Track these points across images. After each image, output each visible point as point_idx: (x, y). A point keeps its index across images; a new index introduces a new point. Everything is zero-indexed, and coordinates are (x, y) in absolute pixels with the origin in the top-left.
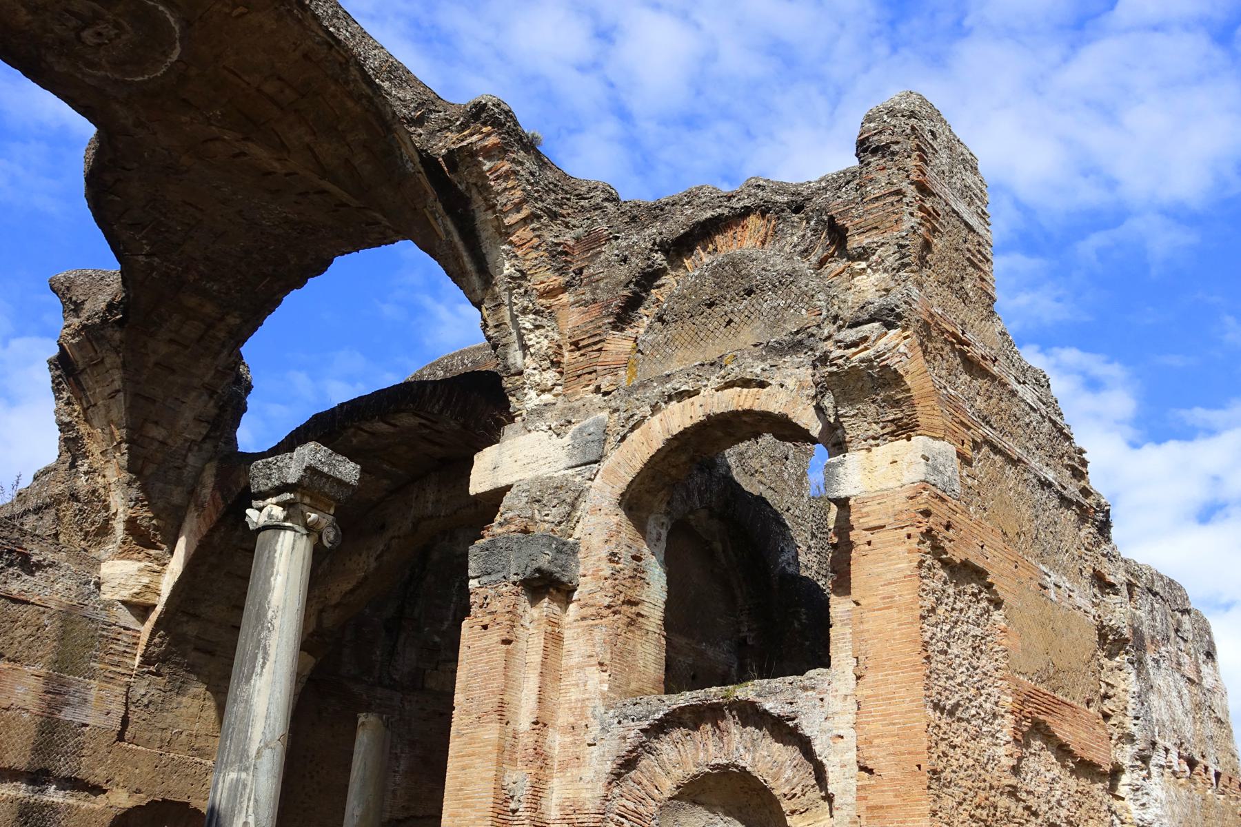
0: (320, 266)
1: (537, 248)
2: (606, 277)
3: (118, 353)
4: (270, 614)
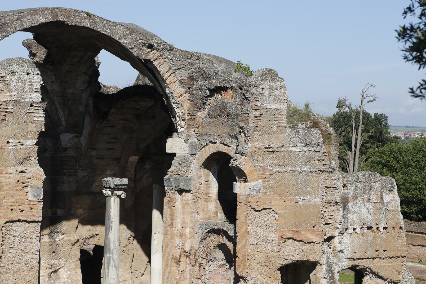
4: (111, 218)
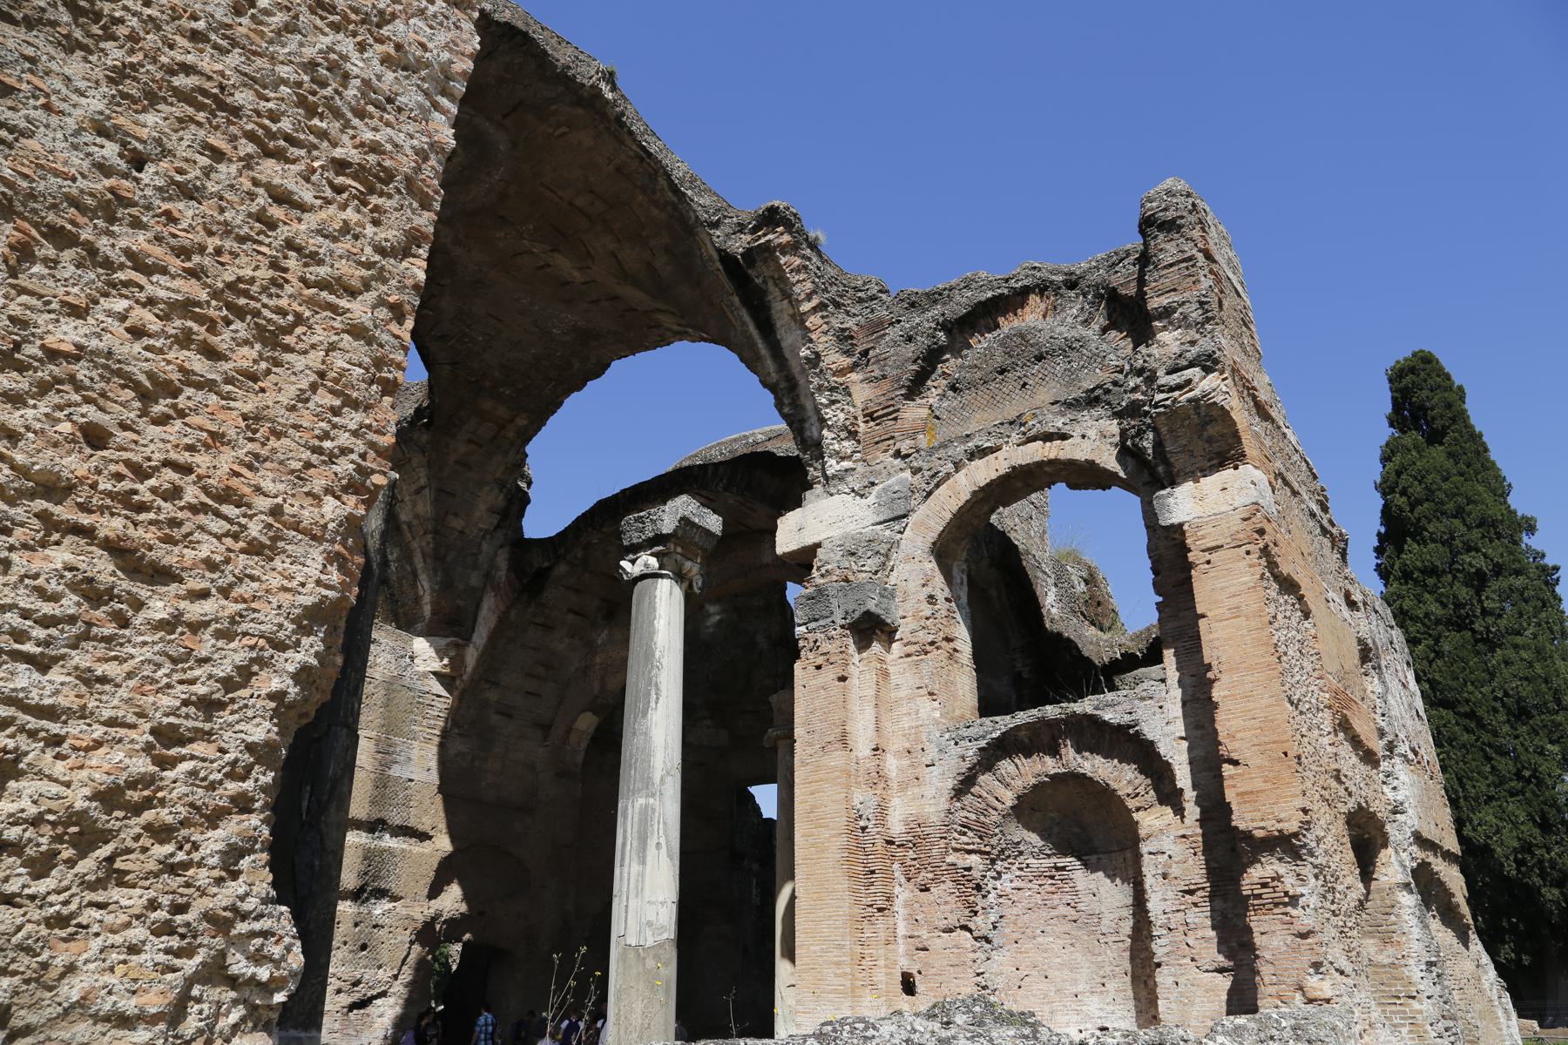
0: (599, 370)
1: (825, 333)
4: (657, 654)
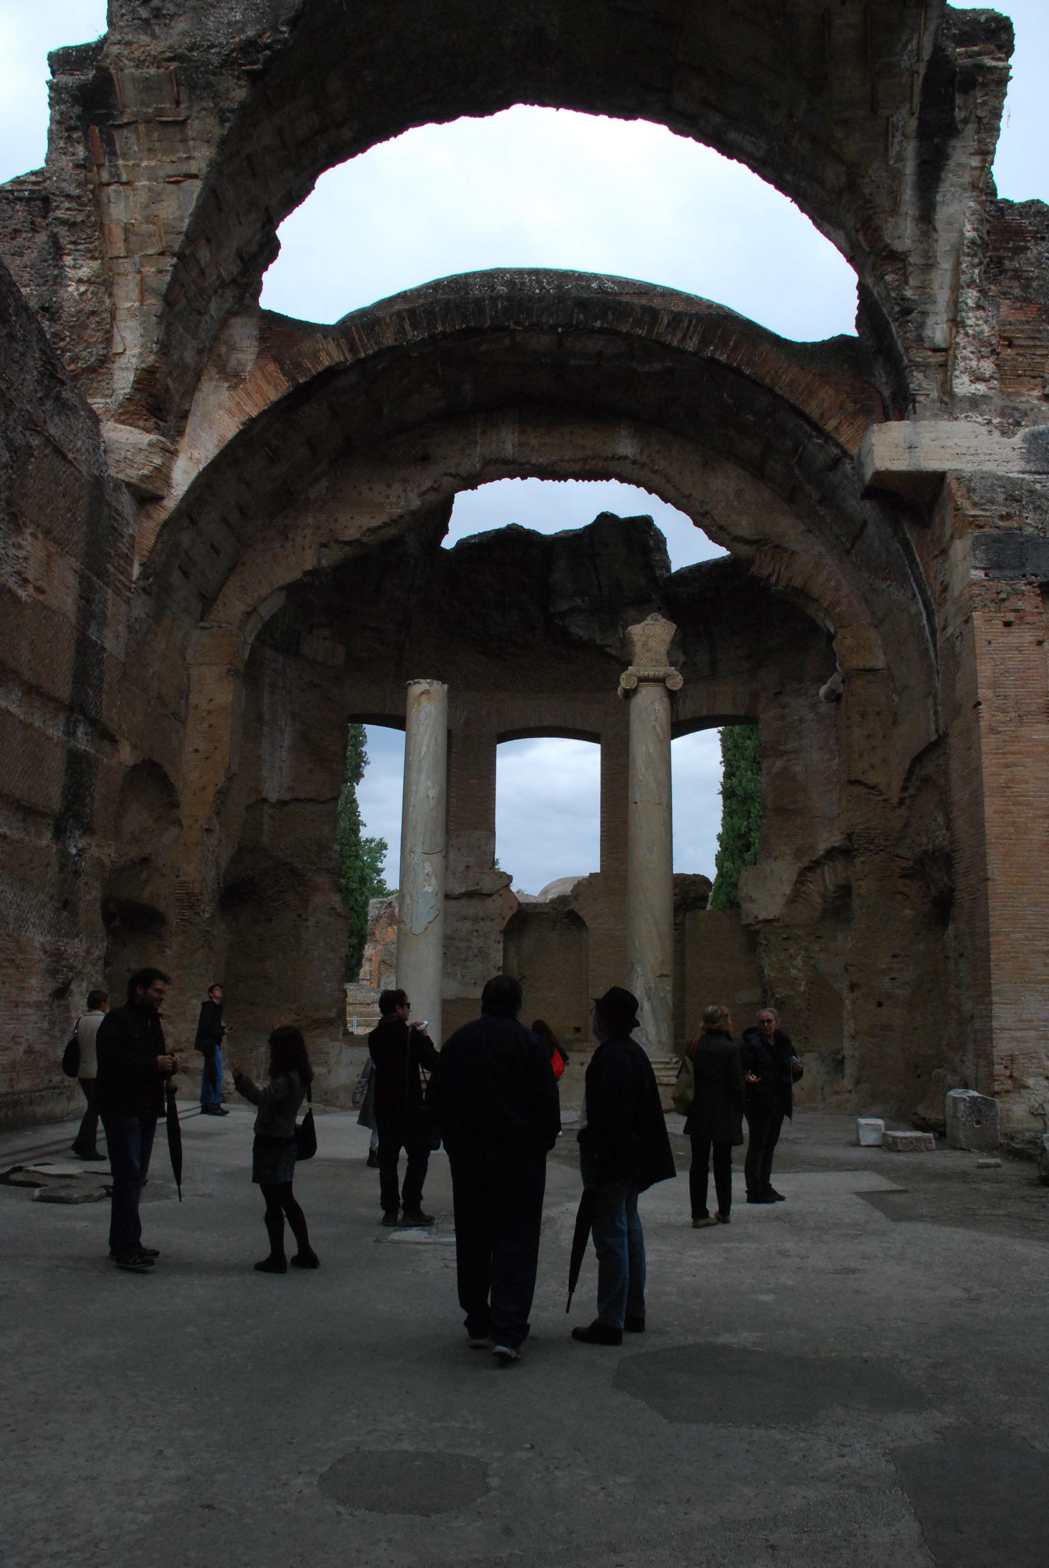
2: (1038, 278)
3: (223, 121)
